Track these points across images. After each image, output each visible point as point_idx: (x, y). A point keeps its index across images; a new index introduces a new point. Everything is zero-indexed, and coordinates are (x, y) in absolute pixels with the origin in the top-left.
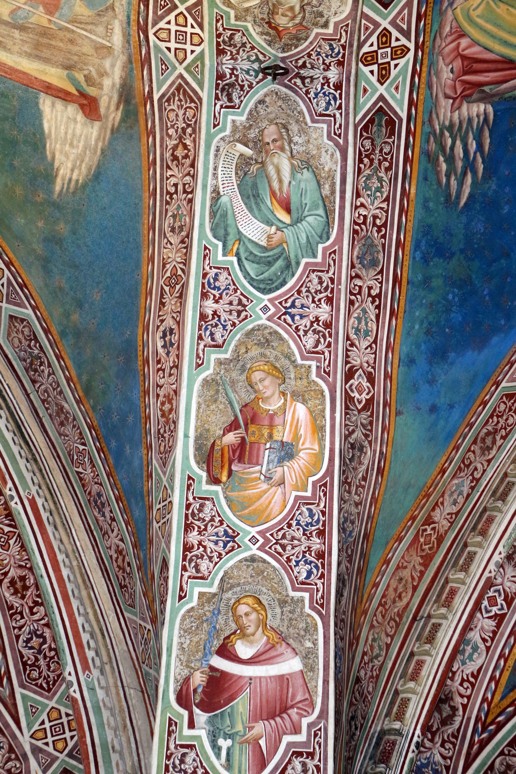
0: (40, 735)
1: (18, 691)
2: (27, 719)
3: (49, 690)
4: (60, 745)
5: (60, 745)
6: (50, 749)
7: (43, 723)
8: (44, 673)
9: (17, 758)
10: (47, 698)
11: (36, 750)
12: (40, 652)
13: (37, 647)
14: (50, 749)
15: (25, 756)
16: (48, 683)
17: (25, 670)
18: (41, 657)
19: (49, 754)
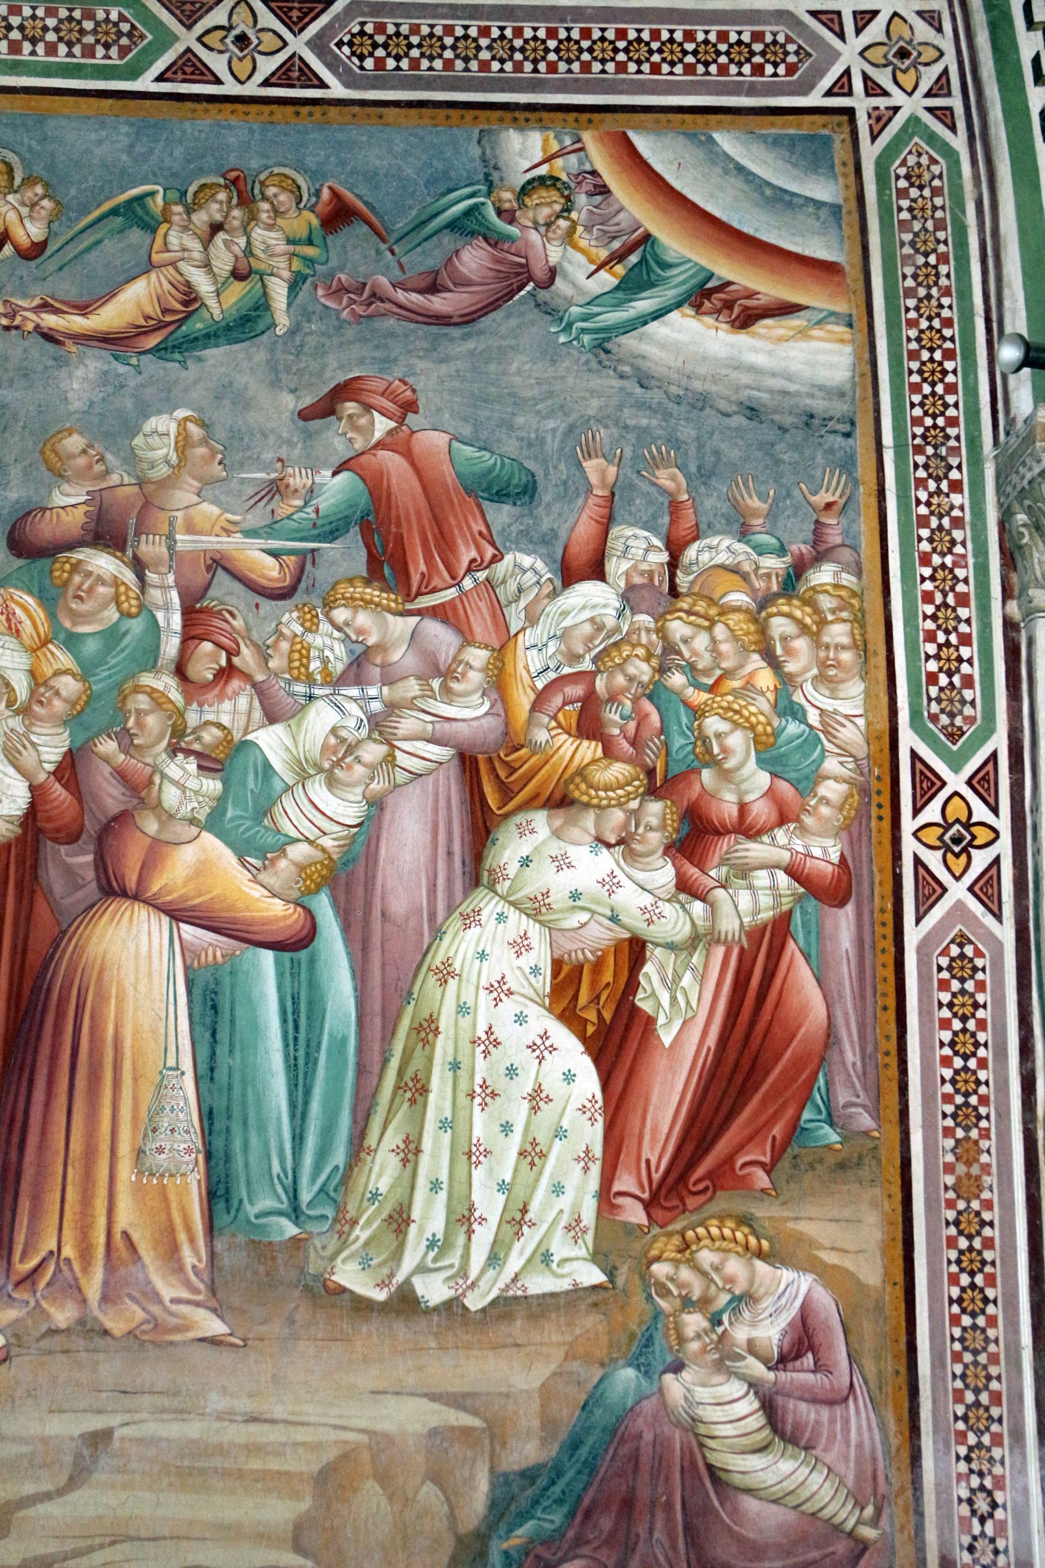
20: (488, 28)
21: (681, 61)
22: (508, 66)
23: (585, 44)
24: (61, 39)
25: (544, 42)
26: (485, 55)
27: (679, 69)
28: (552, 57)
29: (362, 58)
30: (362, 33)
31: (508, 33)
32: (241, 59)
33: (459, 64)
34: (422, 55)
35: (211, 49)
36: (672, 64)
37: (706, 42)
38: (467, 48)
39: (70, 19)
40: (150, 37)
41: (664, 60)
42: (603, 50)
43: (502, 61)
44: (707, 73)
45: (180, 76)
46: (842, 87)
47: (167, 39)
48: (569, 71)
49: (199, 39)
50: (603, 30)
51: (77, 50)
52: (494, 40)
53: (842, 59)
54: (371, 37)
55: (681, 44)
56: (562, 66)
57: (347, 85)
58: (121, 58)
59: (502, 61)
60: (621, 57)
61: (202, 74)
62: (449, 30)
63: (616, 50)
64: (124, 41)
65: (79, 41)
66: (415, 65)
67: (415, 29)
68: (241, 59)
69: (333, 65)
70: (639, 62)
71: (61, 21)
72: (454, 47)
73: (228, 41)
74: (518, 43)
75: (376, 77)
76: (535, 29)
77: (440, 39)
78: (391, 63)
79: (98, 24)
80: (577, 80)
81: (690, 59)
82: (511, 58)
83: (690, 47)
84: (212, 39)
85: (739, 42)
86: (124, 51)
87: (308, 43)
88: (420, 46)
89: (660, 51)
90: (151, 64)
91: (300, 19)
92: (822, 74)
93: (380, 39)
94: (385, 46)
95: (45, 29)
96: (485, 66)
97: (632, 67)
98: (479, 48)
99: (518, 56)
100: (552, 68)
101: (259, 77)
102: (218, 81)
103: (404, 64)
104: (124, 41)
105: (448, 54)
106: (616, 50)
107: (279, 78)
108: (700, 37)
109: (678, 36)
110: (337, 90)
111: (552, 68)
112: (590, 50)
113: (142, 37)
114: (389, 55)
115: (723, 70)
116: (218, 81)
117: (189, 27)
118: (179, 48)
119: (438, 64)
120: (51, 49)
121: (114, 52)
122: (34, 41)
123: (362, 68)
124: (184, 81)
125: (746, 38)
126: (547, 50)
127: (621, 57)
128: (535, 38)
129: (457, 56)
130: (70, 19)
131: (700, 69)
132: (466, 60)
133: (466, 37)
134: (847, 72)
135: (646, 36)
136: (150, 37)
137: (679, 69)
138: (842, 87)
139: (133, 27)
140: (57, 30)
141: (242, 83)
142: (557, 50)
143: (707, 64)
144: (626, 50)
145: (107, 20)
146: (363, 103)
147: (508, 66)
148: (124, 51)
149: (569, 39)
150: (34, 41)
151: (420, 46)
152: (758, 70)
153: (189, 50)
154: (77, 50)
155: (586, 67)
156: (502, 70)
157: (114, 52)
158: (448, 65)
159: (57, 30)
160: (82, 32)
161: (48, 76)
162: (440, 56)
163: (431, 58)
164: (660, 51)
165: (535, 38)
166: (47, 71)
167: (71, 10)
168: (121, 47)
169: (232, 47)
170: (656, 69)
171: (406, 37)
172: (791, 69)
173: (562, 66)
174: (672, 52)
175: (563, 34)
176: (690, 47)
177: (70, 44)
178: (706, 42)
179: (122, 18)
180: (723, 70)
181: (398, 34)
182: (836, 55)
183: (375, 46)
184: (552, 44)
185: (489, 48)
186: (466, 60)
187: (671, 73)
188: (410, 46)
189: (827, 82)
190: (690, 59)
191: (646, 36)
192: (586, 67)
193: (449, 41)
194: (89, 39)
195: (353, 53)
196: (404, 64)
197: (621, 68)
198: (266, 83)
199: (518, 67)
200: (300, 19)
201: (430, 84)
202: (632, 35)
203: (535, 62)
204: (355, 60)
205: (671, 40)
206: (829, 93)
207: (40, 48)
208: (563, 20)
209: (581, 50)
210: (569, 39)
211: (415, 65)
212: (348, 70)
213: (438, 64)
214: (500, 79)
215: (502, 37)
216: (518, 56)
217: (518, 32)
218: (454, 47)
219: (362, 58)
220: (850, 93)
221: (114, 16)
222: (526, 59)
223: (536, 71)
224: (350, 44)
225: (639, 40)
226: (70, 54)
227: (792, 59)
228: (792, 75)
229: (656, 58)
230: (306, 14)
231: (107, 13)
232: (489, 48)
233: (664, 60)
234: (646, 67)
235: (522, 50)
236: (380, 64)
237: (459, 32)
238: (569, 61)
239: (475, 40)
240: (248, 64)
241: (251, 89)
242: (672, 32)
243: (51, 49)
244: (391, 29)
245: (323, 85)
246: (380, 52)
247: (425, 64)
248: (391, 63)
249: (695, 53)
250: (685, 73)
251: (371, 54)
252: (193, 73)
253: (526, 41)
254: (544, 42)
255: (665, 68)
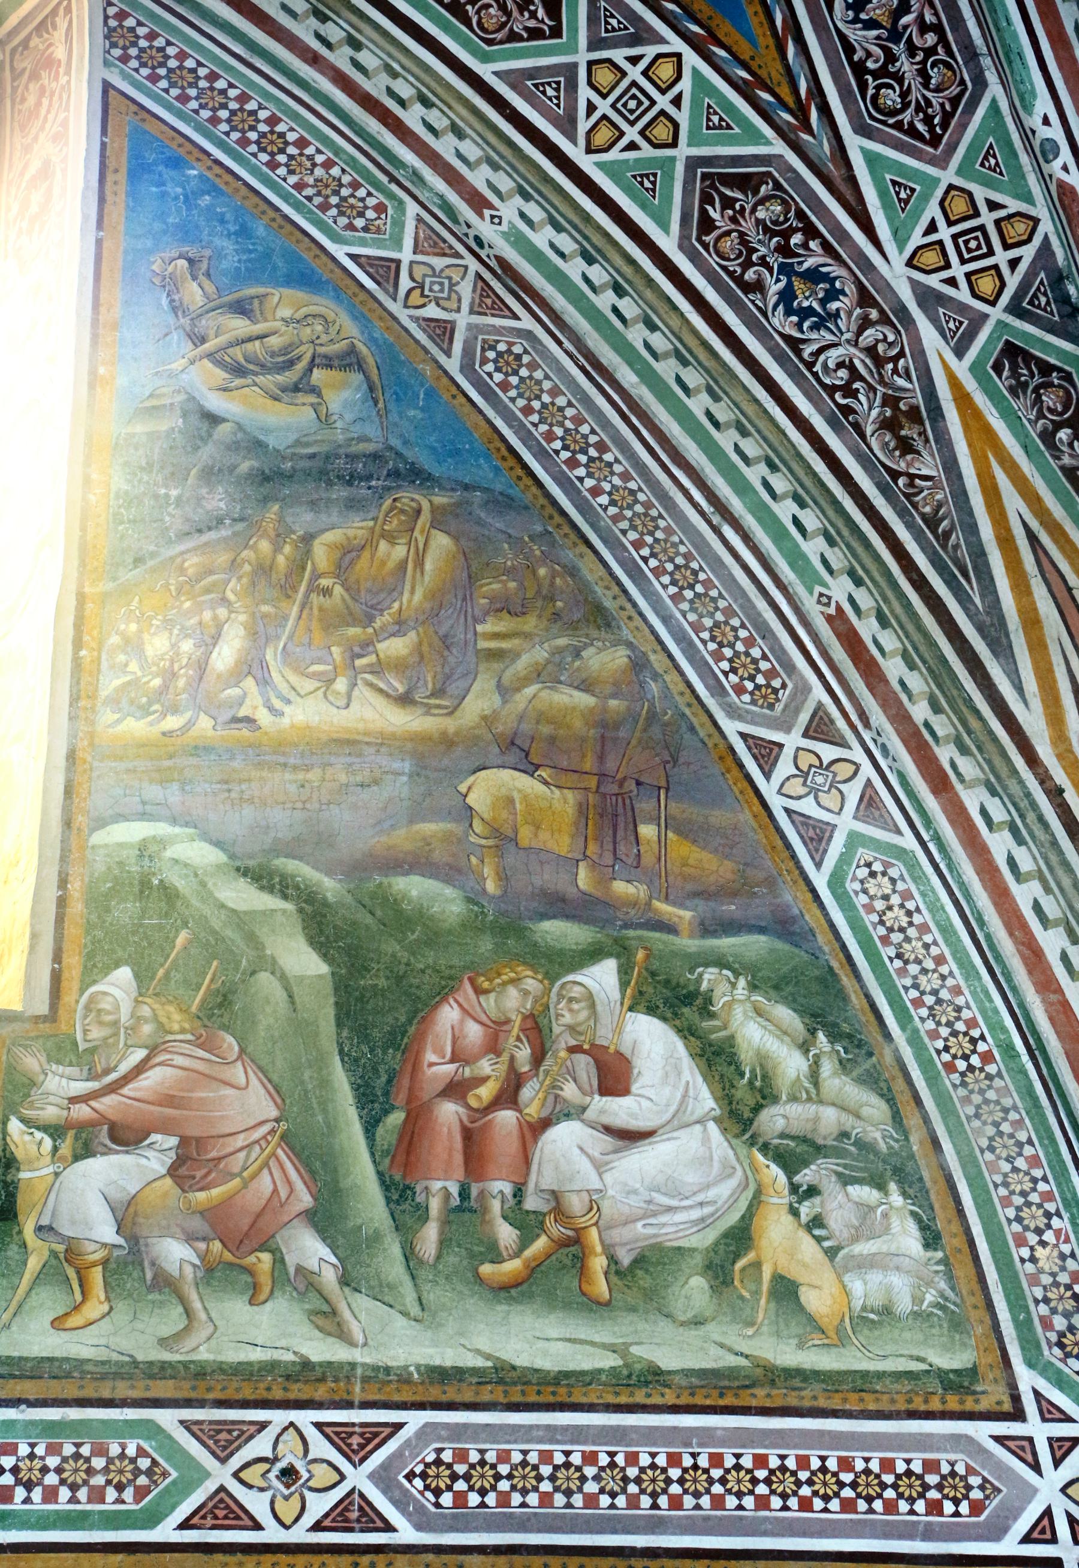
0: (931, 258)
1: (854, 143)
2: (890, 220)
3: (935, 141)
4: (987, 285)
5: (987, 285)
6: (963, 294)
7: (932, 228)
8: (915, 95)
9: (884, 320)
10: (932, 161)
11: (928, 298)
12: (895, 35)
13: (885, 21)
14: (963, 294)
15: (902, 311)
16: (928, 120)
17: (863, 87)
18: (899, 49)
19: (963, 308)
20: (595, 1454)
21: (837, 1495)
22: (621, 1501)
23: (716, 1473)
24: (63, 1482)
25: (664, 1470)
26: (591, 1487)
27: (834, 1505)
28: (675, 1489)
29: (437, 1492)
30: (438, 1462)
31: (620, 1460)
32: (286, 1498)
33: (559, 1499)
34: (513, 1488)
35: (250, 1487)
36: (826, 1498)
37: (867, 1472)
38: (568, 1479)
39: (77, 1456)
40: (174, 1474)
41: (815, 1493)
42: (739, 1481)
43: (613, 1495)
44: (871, 1511)
45: (209, 1521)
46: (1043, 1532)
47: (195, 1475)
48: (698, 1507)
49: (236, 1475)
50: (738, 1456)
51: (82, 1494)
52: (602, 1469)
53: (1039, 1497)
54: (449, 1466)
55: (835, 1474)
56: (689, 1501)
57: (419, 1527)
58: (137, 1501)
59: (613, 1495)
60: (762, 1489)
61: (238, 1518)
62: (546, 1457)
63: (755, 1481)
64: (143, 1480)
65: (85, 1482)
66: (504, 1500)
67: (504, 1456)
68: (286, 1498)
69: (401, 1503)
70: (784, 1496)
71: (65, 1460)
72: (552, 1478)
73: (272, 1475)
74: (632, 1472)
75: (455, 1516)
76: (653, 1455)
77: (535, 1468)
78: (474, 1499)
79: (110, 1461)
80: (707, 1518)
81: (847, 1493)
82: (624, 1490)
83: (847, 1477)
84: (252, 1475)
85: (909, 1473)
86: (141, 1493)
87: (371, 1476)
88: (510, 1477)
89: (810, 1482)
90: (173, 1508)
91: (362, 1447)
92: (1016, 1514)
93: (461, 1469)
94: (467, 1477)
95: (45, 1470)
96: (591, 1501)
97: (776, 1502)
98: (583, 1479)
99: (633, 1489)
100: (676, 1503)
101: (308, 1520)
102: (258, 1527)
103: (491, 1499)
104: (143, 1480)
105: (546, 1486)
106: (755, 1481)
107: (334, 1521)
108: (860, 1465)
109: (832, 1464)
110: (406, 1534)
111: (676, 1503)
112: (723, 1481)
113: (165, 1474)
114: (471, 1488)
115: (890, 1507)
116: (258, 1527)
117: (223, 1461)
118: (211, 1486)
119: (533, 1499)
120: (50, 1495)
121: (128, 1494)
122: (29, 1486)
123: (437, 1505)
124: (214, 1527)
125: (917, 1467)
126: (668, 1481)
127: (762, 1489)
128: (653, 1466)
129: (557, 1489)
130: (77, 1456)
131: (862, 1505)
132: (568, 1493)
133: (567, 1465)
134: (1048, 1513)
135: (791, 1463)
136: (174, 1474)
137: (834, 1505)
138: (1043, 1532)
139: (154, 1462)
140: (59, 1470)
141: (287, 1527)
142: (681, 1481)
143: (869, 1499)
144: (768, 1481)
145: (122, 1456)
146: (439, 1549)
147: (621, 1501)
148: (141, 1493)
149: (695, 1467)
150: (29, 1486)
151: (510, 1477)
152: (935, 1508)
153: (222, 1489)
154: (82, 1494)
155: (718, 1502)
156: (612, 1506)
157: (128, 1494)
158: (546, 1500)
159: (59, 1470)
160: (90, 1471)
161: (44, 1528)
162: (536, 1489)
163: (524, 1492)
164: (810, 1482)
165: (653, 1466)
166: (44, 1522)
167: (78, 1445)
168: (137, 1489)
169: (277, 1484)
170: (805, 1505)
171: (493, 1466)
172: (977, 1508)
173: (689, 1501)
174: (825, 1484)
175: (688, 1462)
176: (847, 1477)
177: (74, 1488)
178: (867, 1472)
179: (141, 1452)
180: (890, 1507)
181: (482, 1463)
182: (1035, 1491)
183: (454, 1477)
184: (675, 1473)
185: (597, 1478)
186: (568, 1493)
187: (825, 1510)
188: (498, 1477)
189: (1023, 1525)
190: (847, 1493)
191: (791, 1463)
192: (718, 1502)
193: (546, 1470)
194: (99, 1480)
195: (427, 1487)
196: (491, 1499)
197: (762, 1503)
198: (317, 1527)
199: (633, 1503)
200: (362, 1447)
201: (523, 1525)
202: (774, 1462)
203: (654, 1495)
204: (429, 1495)
205: (823, 1469)
206: (1027, 1539)
207: (37, 1494)
208: (688, 1444)
209: (711, 1481)
210: (695, 1467)
211: (504, 1500)
212: (421, 1509)
213: (533, 1499)
214: (611, 1518)
215: (613, 1465)
216: (633, 1489)
217: (632, 1459)
218: (552, 1478)
219: (437, 1492)
220: (1054, 1540)
221: (131, 1451)
222: (643, 1491)
223: (655, 1506)
224: (424, 1476)
225: (783, 1469)
226: (73, 1500)
227: (976, 1494)
228: (978, 1515)
229: (805, 1491)
230: (369, 1441)
231: (123, 1447)
232: (597, 1478)
233: (815, 1493)
234: (793, 1502)
235: (638, 1481)
236: (460, 1500)
237: (559, 1459)
238: (697, 1495)
239: (579, 1469)
240: (295, 1503)
241: (299, 1535)
242: (823, 1459)
243: (50, 1495)
244: (474, 1457)
245: (389, 1528)
246: (461, 1486)
247: (516, 1499)
248: (474, 1499)
249: (854, 1485)
250: (843, 1510)
251: (449, 1488)
252: (226, 1517)
253: (642, 1470)
254: (664, 1470)
255: (818, 1504)
